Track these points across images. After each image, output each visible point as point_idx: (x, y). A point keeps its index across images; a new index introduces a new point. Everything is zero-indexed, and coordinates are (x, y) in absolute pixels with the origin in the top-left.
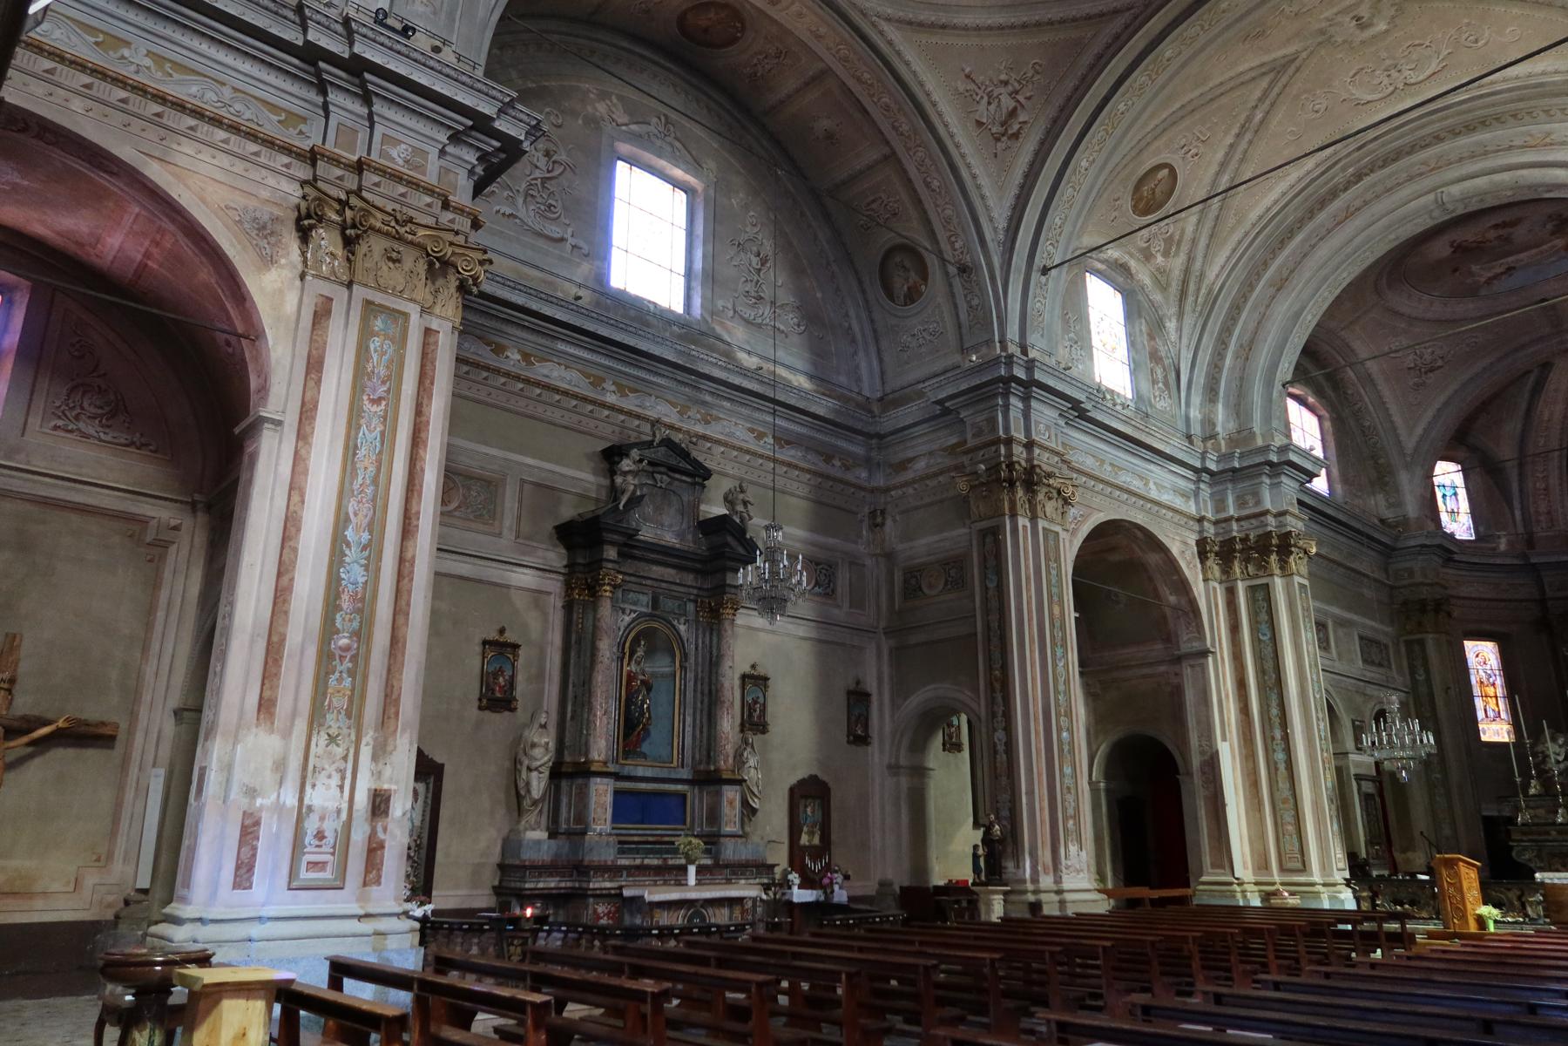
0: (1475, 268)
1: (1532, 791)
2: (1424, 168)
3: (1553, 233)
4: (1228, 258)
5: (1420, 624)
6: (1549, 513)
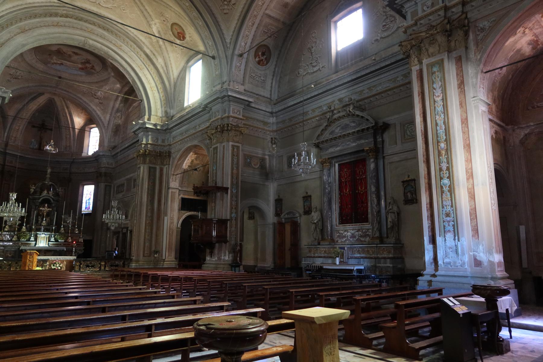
0: (54, 58)
2: (86, 29)
3: (82, 63)
4: (10, 8)
6: (15, 137)
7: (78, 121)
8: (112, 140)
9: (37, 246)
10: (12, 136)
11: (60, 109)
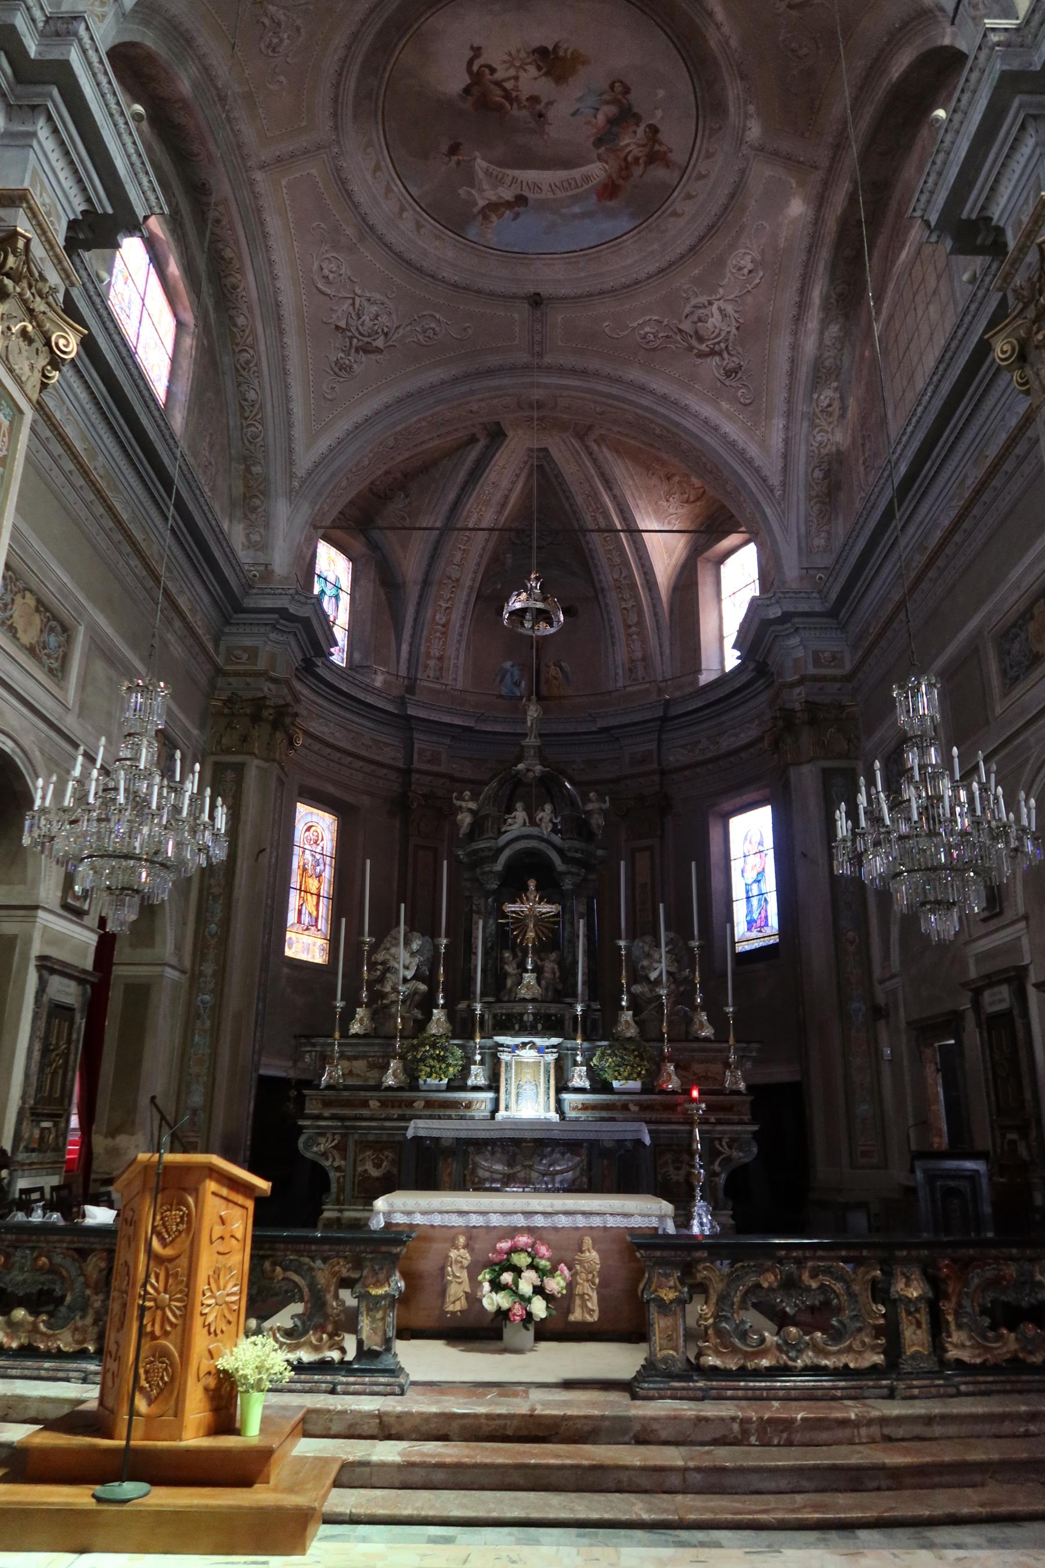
1: (355, 1028)
5: (244, 739)
6: (440, 658)
7: (664, 549)
8: (820, 542)
9: (501, 1115)
10: (428, 656)
11: (579, 500)
